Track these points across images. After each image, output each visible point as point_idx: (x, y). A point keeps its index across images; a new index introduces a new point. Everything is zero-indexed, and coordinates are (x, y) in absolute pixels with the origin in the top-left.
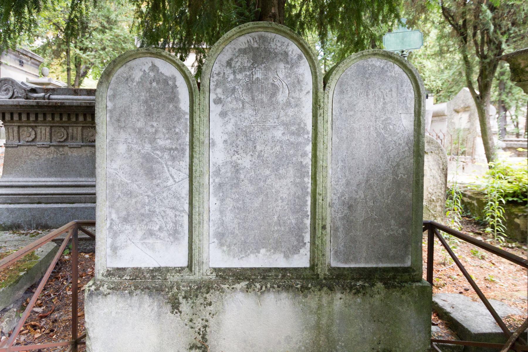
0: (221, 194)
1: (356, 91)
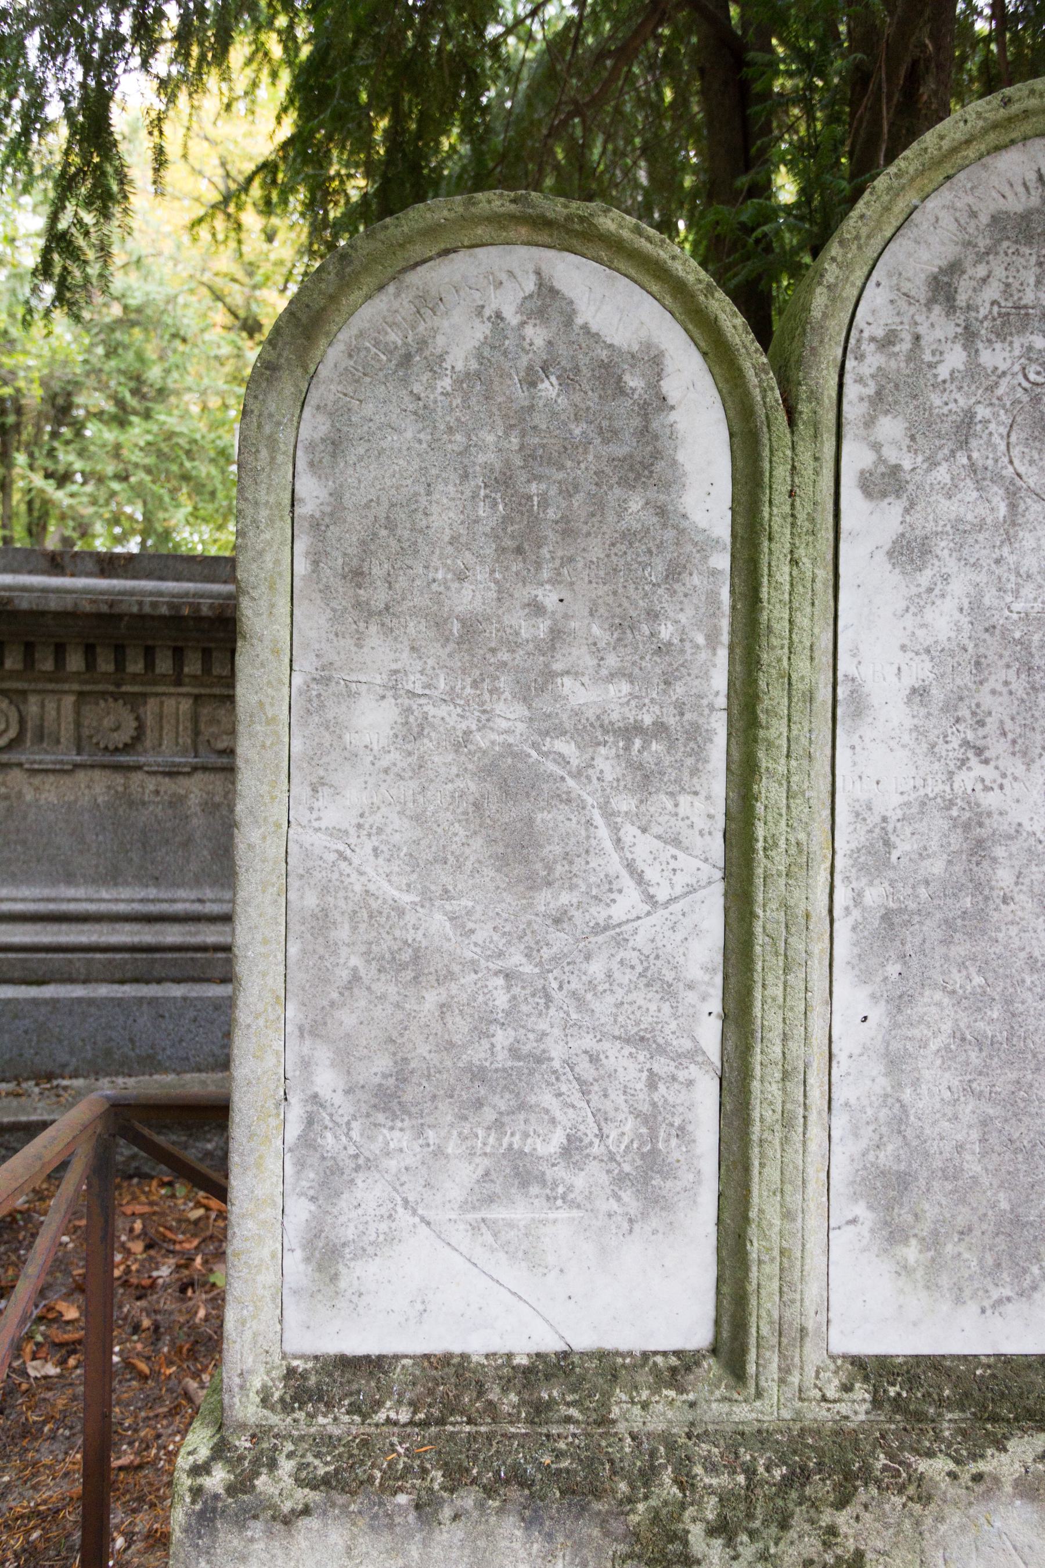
0: (893, 969)
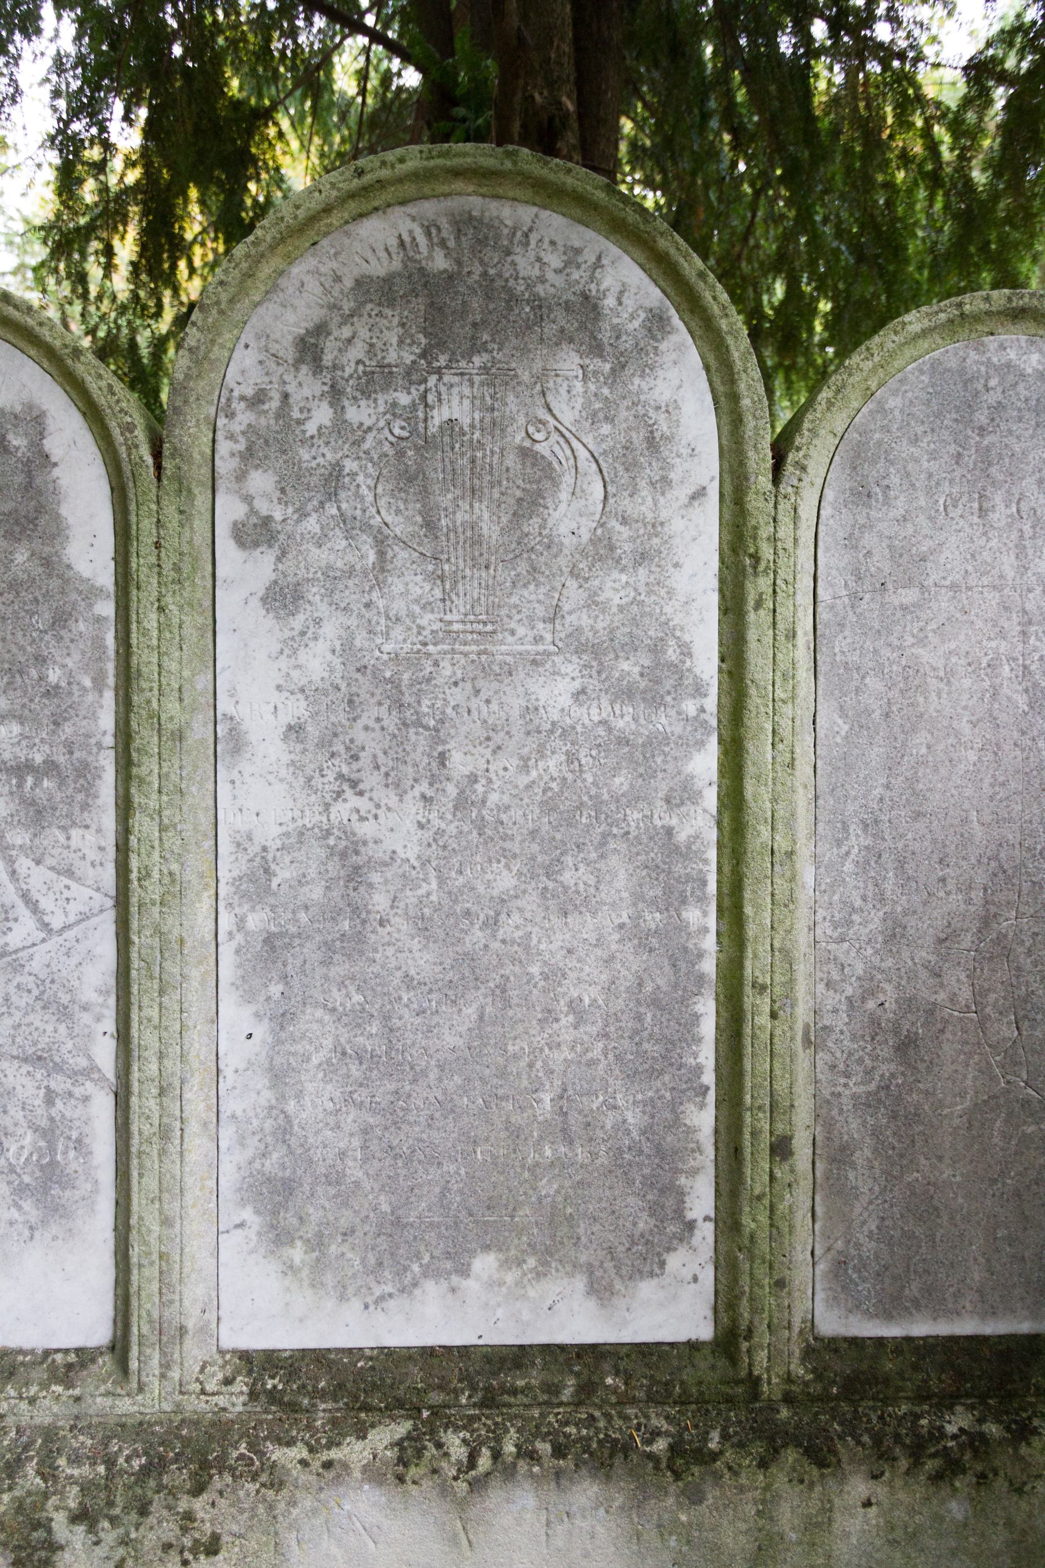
0: (276, 990)
1: (929, 492)
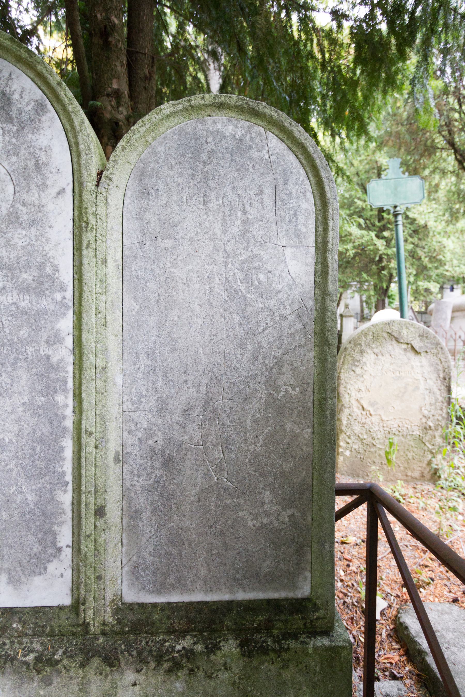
1: (178, 193)
